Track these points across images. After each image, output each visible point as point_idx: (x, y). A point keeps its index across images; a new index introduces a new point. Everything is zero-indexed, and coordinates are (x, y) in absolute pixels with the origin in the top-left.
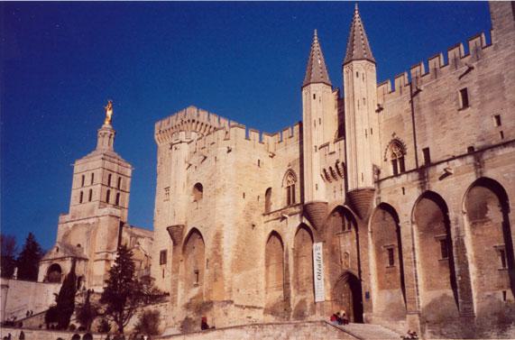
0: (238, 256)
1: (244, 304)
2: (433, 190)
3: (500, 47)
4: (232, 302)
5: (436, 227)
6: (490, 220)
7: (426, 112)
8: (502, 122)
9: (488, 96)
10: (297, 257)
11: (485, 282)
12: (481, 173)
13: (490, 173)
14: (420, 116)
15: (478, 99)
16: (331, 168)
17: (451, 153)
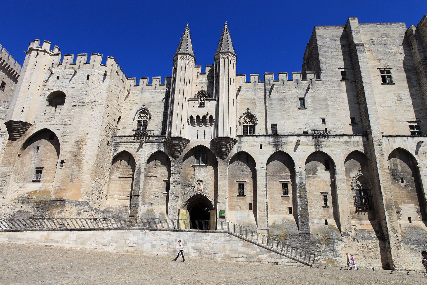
0: (97, 164)
1: (94, 207)
2: (285, 150)
3: (326, 84)
4: (88, 204)
5: (281, 175)
6: (318, 176)
7: (275, 103)
8: (326, 122)
9: (318, 106)
10: (146, 176)
11: (313, 213)
12: (319, 148)
13: (324, 149)
14: (271, 104)
15: (312, 106)
16: (198, 117)
17: (293, 131)
